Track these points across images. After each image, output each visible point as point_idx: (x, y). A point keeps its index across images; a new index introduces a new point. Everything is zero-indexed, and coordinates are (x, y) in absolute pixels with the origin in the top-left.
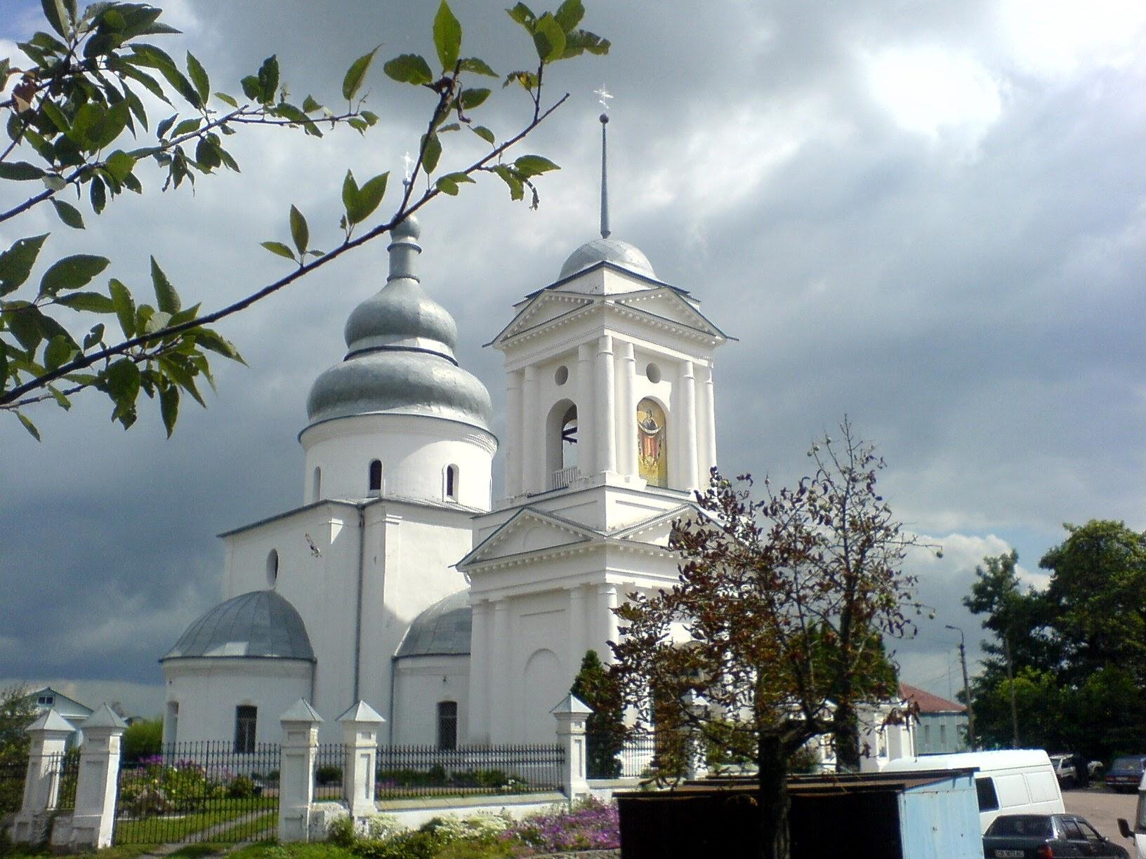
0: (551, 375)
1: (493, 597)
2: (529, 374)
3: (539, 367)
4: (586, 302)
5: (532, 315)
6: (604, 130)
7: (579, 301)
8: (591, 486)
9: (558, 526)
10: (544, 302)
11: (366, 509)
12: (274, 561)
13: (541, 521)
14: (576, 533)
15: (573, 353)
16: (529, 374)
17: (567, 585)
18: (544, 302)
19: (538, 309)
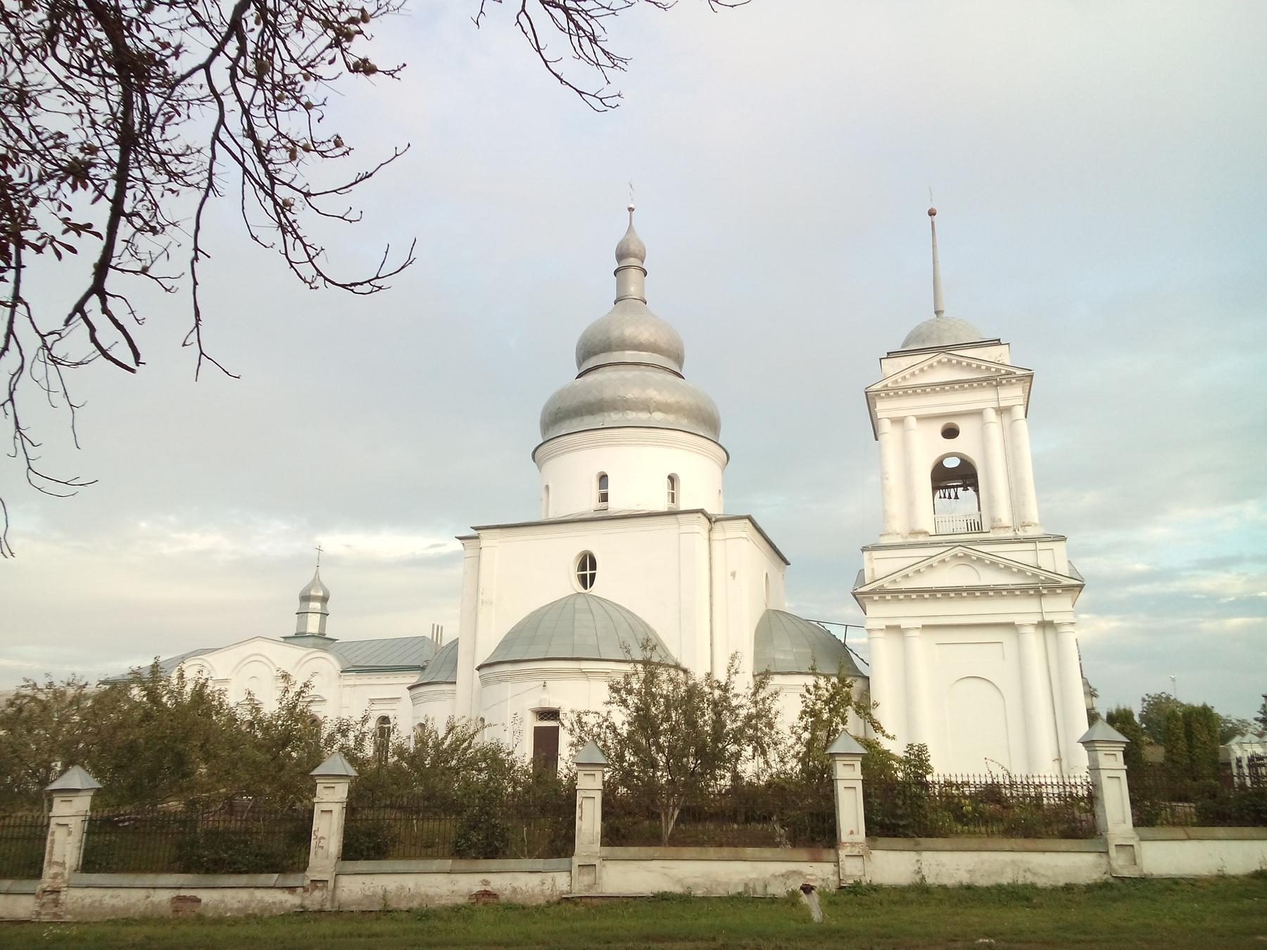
0: (938, 427)
1: (904, 624)
2: (912, 422)
3: (920, 419)
4: (1003, 372)
5: (922, 370)
6: (933, 223)
7: (993, 370)
8: (1021, 534)
9: (1007, 568)
10: (940, 362)
11: (717, 523)
12: (587, 564)
13: (979, 559)
14: (1034, 575)
15: (979, 413)
16: (912, 422)
17: (1017, 620)
18: (940, 362)
19: (931, 366)
